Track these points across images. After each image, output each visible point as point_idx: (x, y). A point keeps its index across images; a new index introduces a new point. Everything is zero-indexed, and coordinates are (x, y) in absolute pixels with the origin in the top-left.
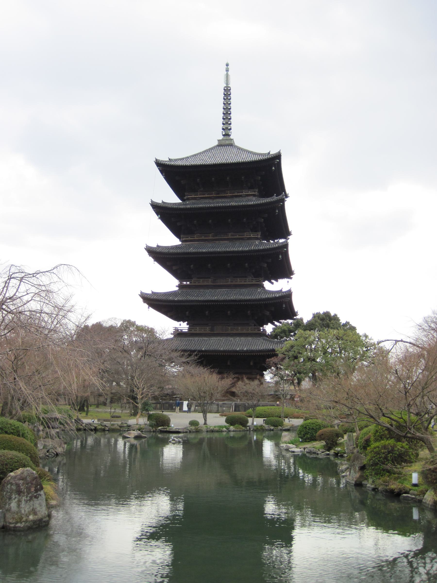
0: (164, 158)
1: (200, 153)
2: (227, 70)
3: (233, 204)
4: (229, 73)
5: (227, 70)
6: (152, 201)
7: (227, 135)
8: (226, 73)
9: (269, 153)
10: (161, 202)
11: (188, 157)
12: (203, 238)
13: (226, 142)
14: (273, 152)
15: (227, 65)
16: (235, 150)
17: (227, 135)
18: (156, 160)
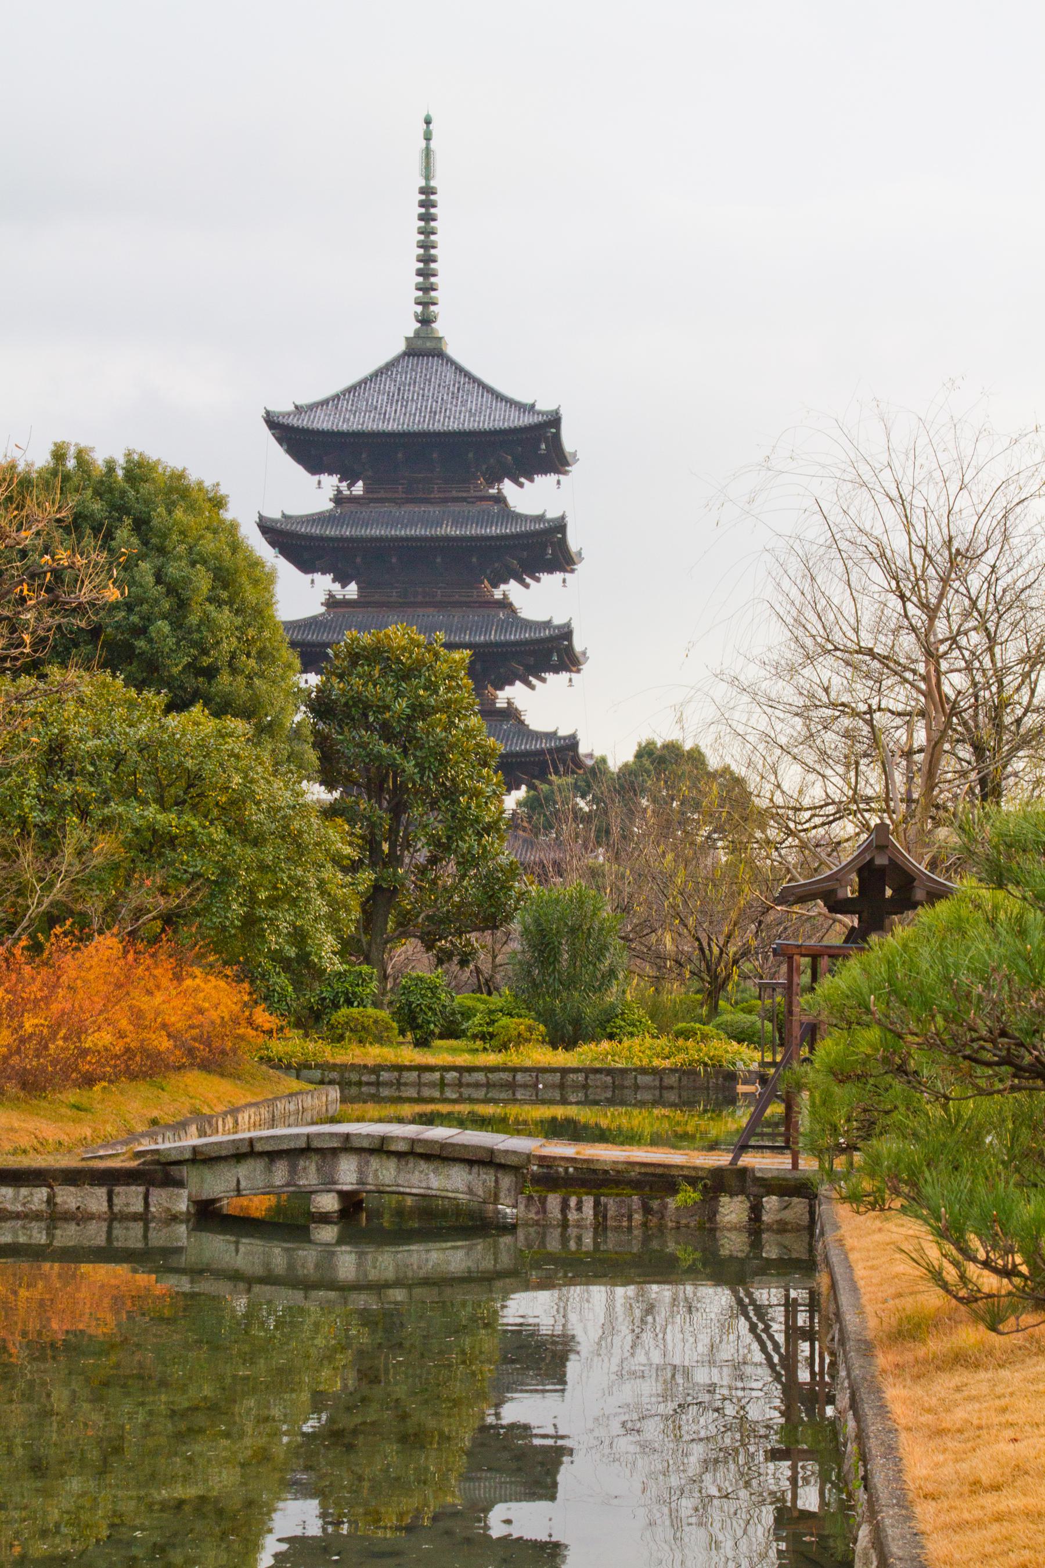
0: (282, 406)
1: (364, 381)
2: (428, 137)
3: (449, 530)
4: (433, 144)
5: (428, 137)
6: (261, 517)
7: (426, 321)
8: (423, 144)
9: (533, 406)
10: (277, 516)
11: (337, 397)
12: (377, 598)
13: (424, 348)
14: (545, 405)
15: (428, 122)
16: (450, 375)
17: (426, 321)
18: (268, 413)
